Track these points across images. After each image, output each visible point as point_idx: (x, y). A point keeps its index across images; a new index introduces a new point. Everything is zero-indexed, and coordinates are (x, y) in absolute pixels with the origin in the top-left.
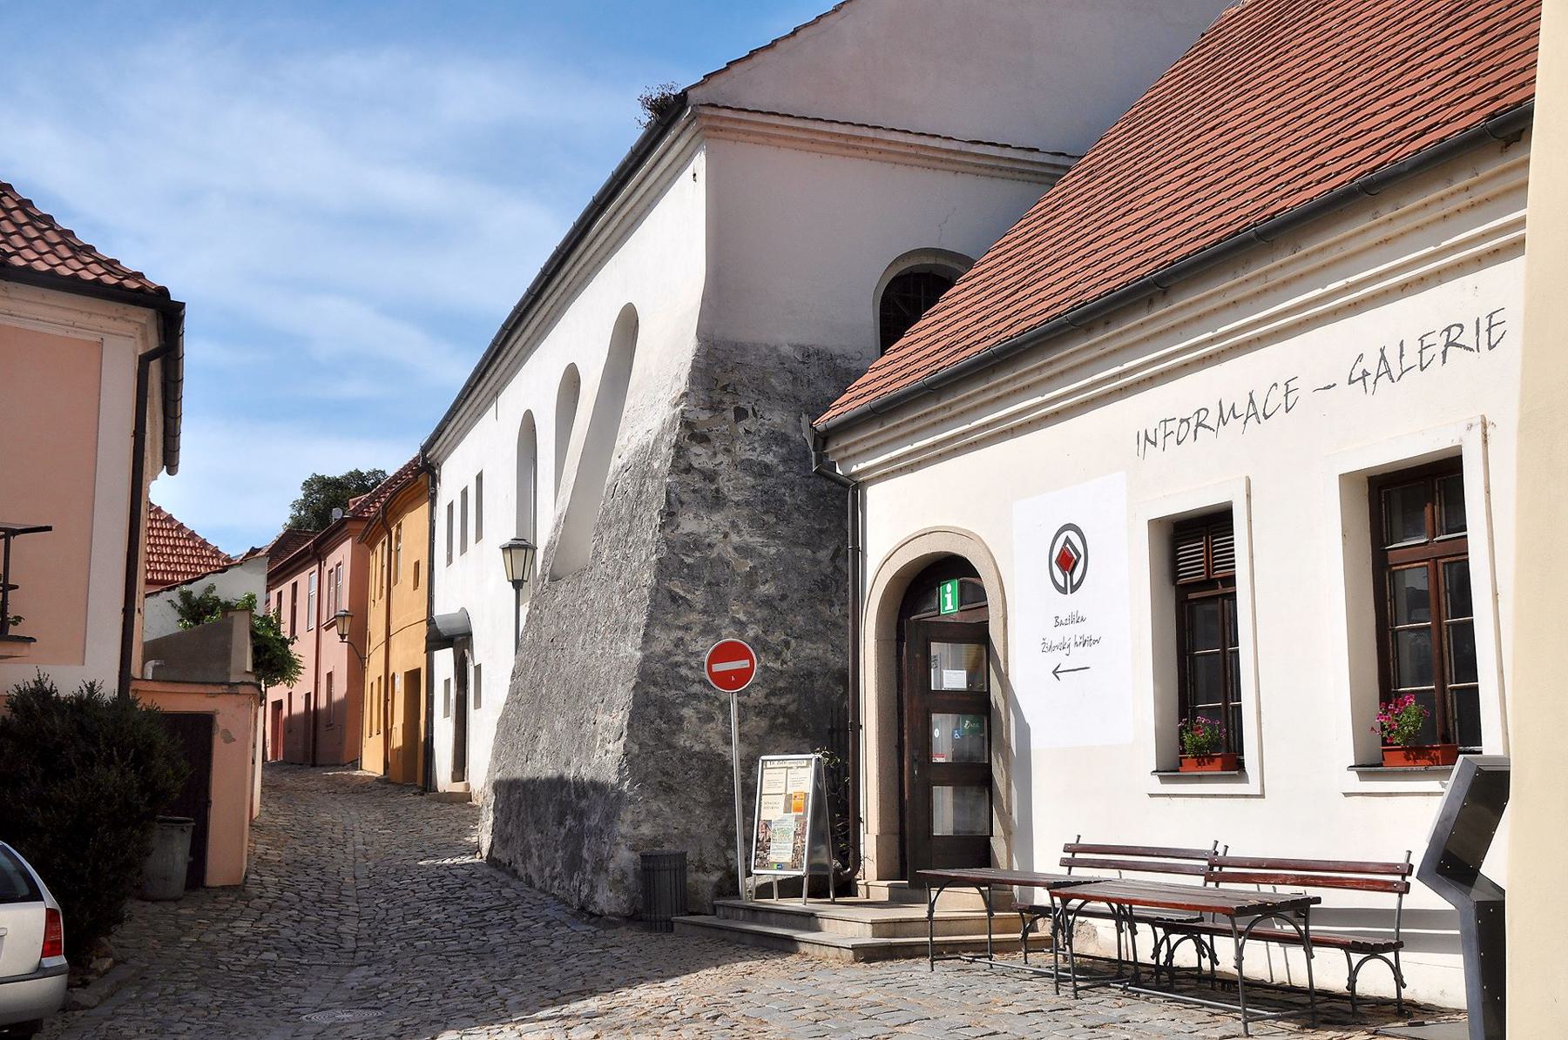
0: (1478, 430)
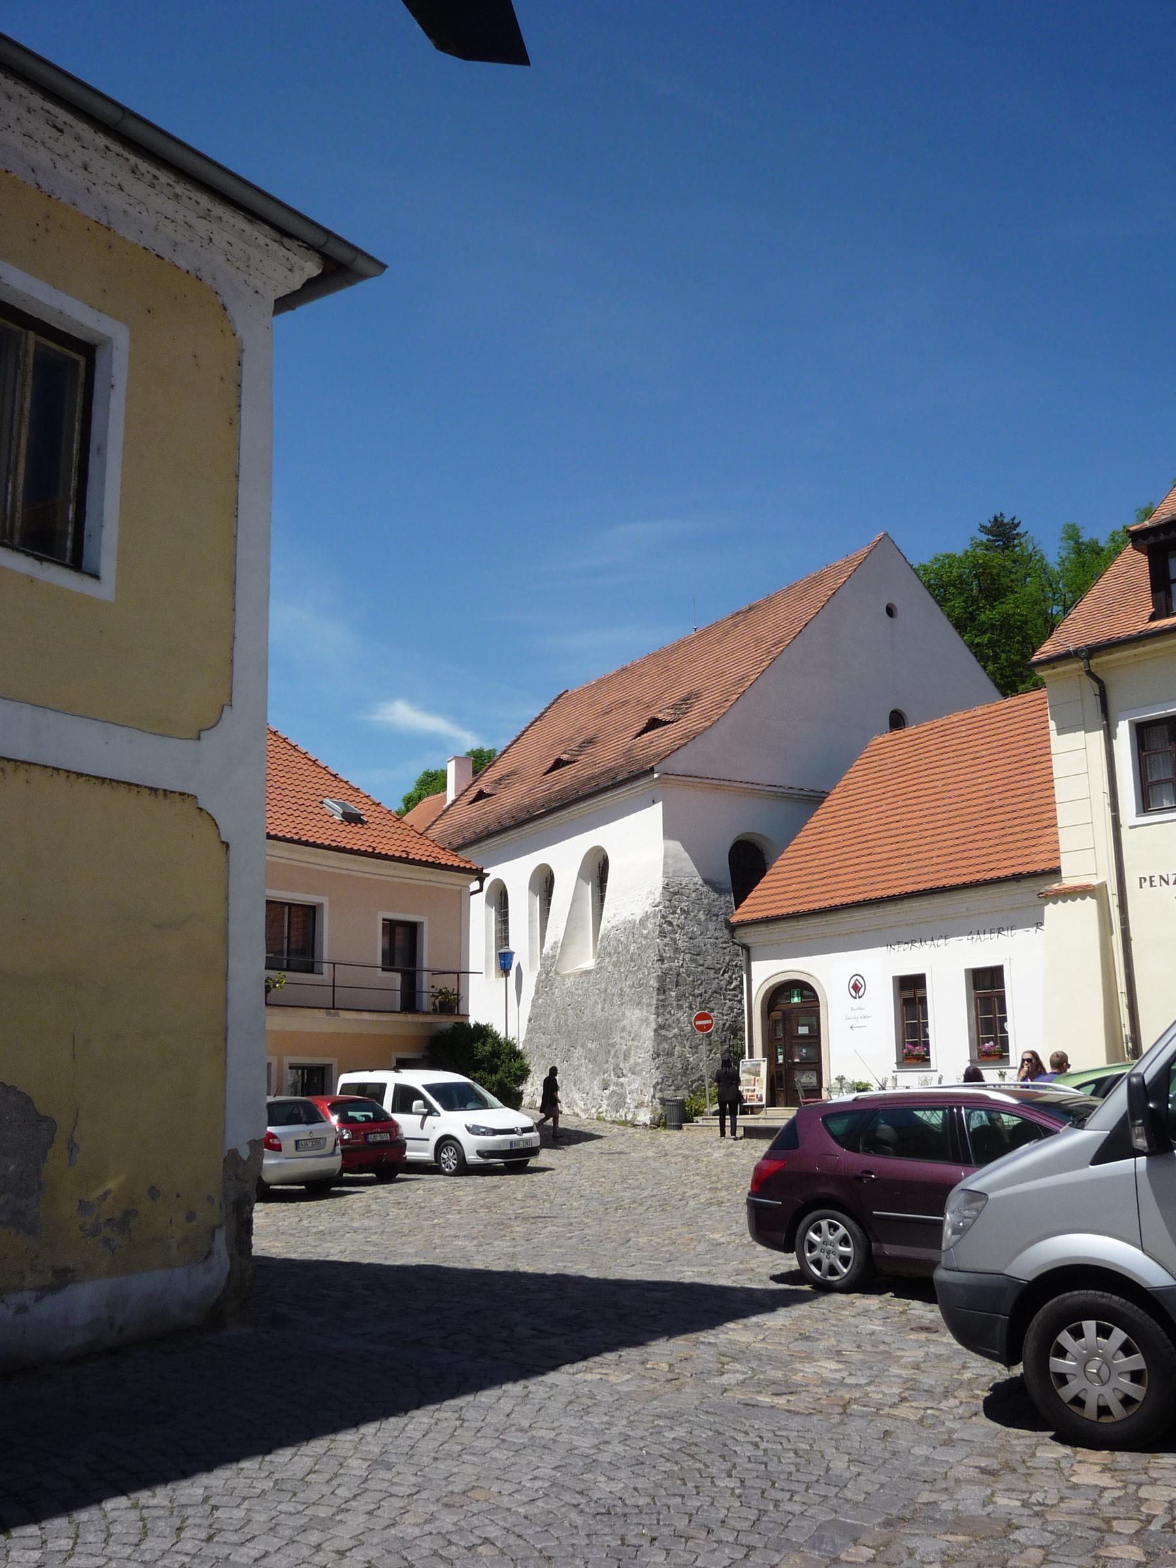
0: (1008, 961)
